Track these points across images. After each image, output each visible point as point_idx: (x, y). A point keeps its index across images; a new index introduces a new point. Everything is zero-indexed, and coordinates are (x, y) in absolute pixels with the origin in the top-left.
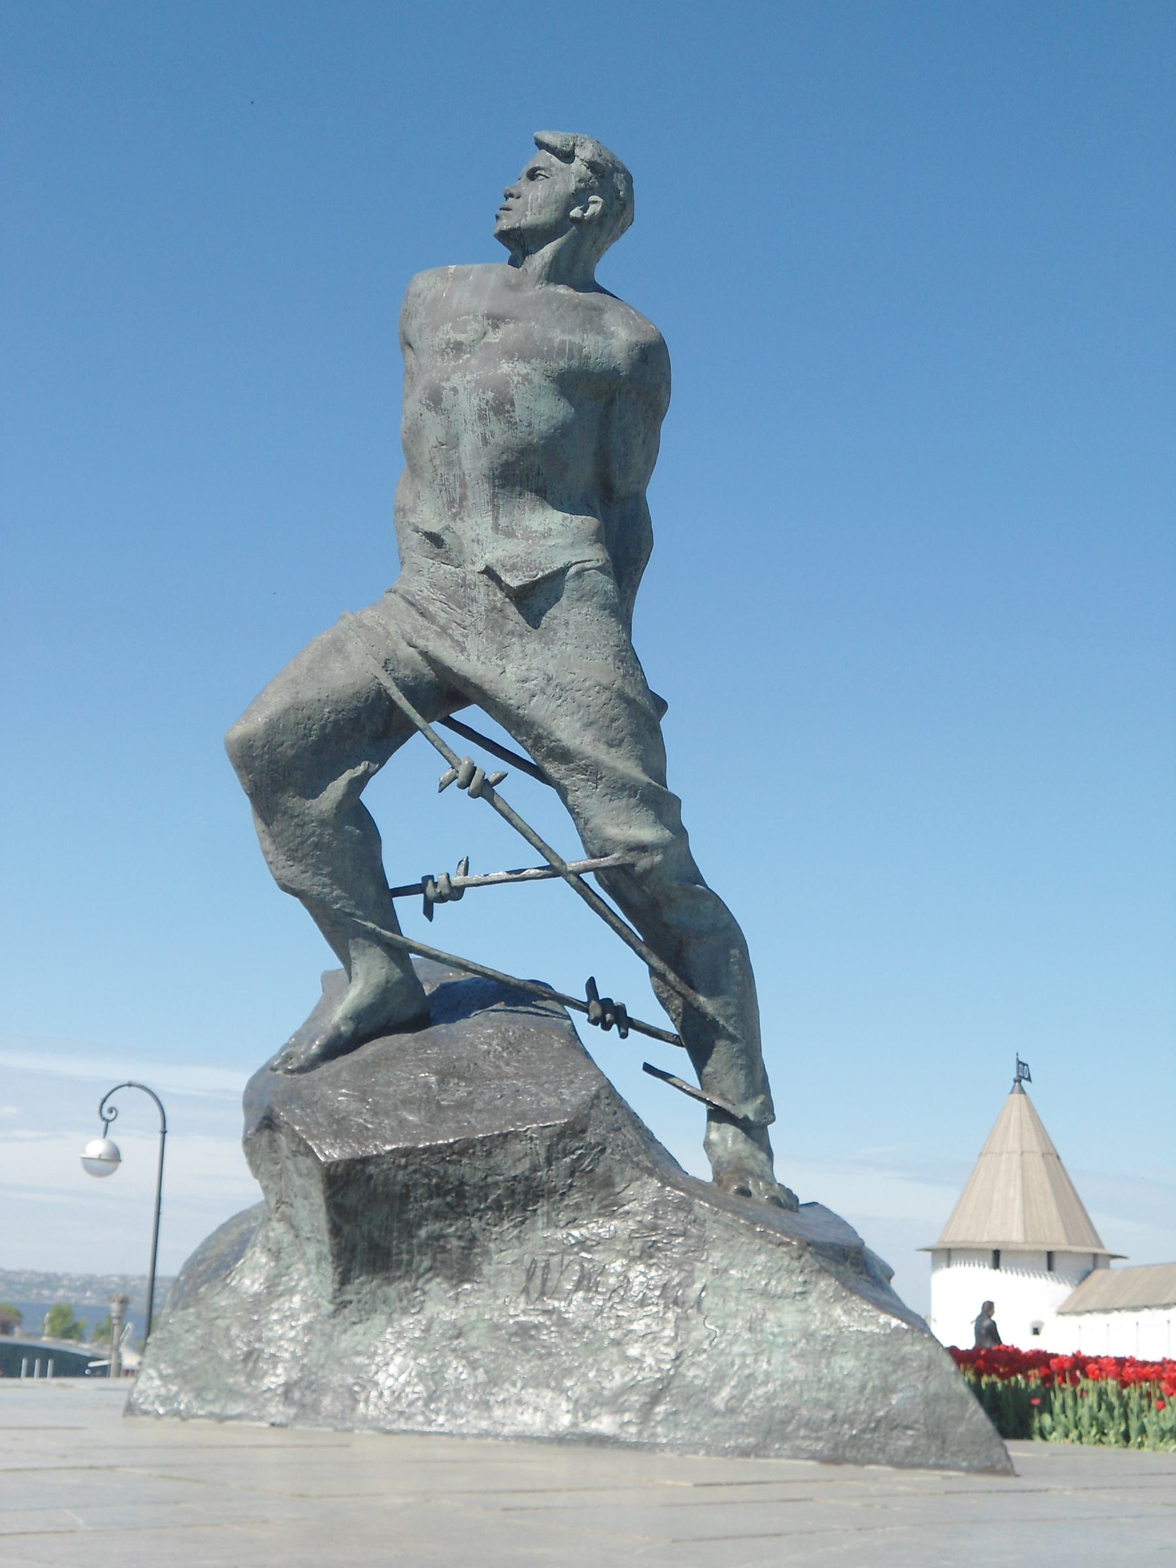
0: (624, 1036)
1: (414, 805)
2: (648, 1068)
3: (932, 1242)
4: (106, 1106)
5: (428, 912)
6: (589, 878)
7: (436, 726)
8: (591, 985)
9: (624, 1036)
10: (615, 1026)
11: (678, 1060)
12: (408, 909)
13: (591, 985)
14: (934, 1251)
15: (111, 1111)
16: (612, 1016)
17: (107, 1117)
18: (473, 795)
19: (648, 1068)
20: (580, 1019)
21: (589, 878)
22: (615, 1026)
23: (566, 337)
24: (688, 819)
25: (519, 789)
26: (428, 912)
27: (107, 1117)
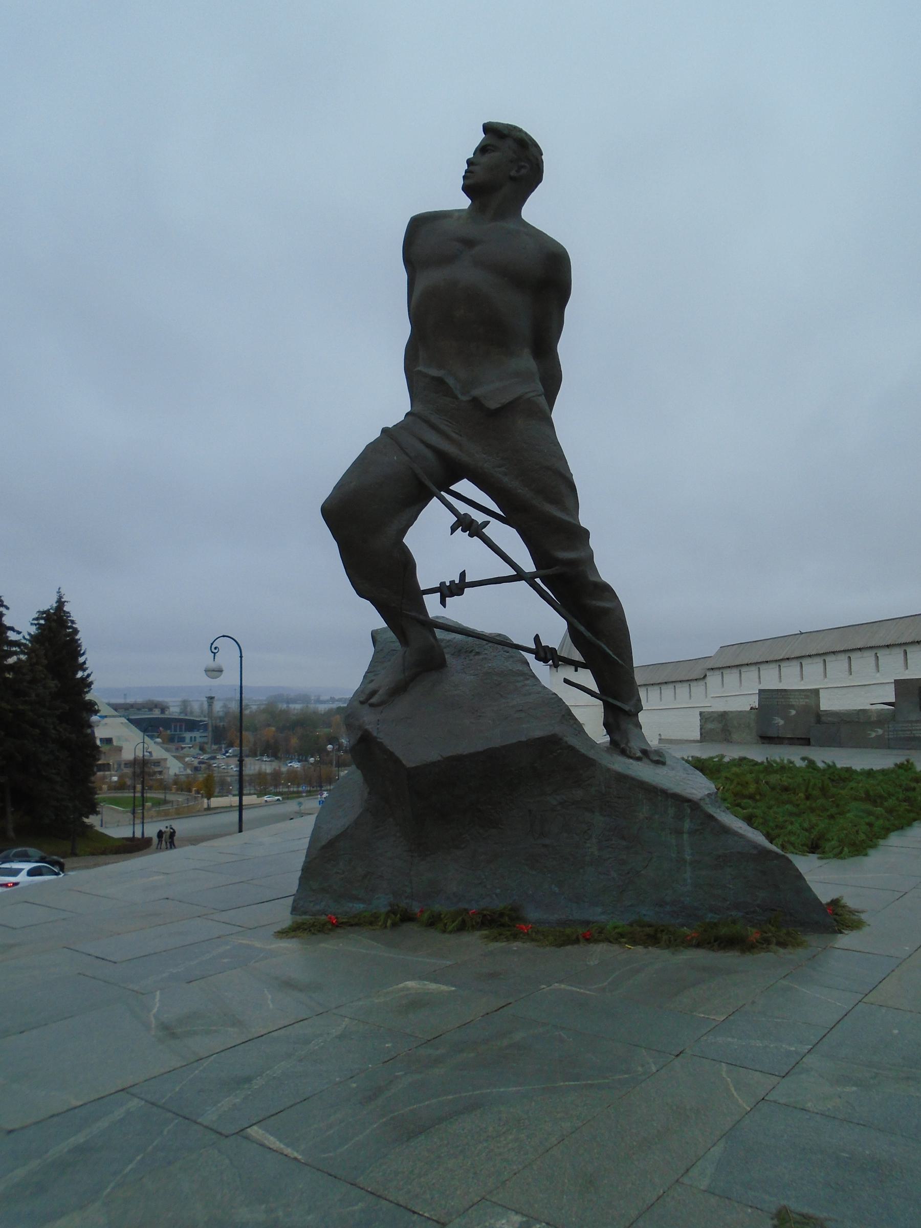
1: (435, 543)
4: (213, 646)
5: (443, 603)
6: (538, 580)
7: (442, 493)
8: (537, 639)
11: (586, 678)
13: (537, 639)
15: (215, 648)
17: (214, 650)
18: (471, 535)
19: (566, 681)
20: (530, 658)
21: (538, 580)
24: (593, 543)
26: (443, 603)
27: (214, 650)
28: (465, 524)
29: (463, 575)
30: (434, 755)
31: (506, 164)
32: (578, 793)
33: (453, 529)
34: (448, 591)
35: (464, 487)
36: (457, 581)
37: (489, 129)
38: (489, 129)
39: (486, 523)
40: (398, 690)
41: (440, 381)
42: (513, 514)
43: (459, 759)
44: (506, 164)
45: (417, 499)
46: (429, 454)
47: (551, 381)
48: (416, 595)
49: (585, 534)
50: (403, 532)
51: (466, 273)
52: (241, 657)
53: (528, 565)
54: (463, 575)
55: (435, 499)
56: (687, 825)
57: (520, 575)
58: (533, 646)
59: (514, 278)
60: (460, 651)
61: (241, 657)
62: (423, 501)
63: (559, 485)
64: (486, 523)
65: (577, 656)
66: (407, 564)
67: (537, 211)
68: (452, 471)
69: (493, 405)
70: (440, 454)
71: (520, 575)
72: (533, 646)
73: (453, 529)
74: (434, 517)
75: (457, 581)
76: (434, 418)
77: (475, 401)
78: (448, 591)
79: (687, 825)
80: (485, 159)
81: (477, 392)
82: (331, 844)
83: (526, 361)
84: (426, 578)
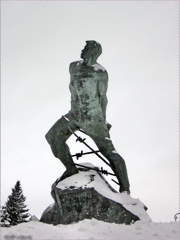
0: (107, 175)
2: (112, 180)
5: (77, 159)
6: (99, 153)
8: (102, 168)
9: (107, 175)
10: (106, 174)
11: (115, 178)
12: (74, 159)
13: (102, 168)
16: (106, 172)
19: (112, 180)
20: (101, 173)
22: (106, 174)
23: (90, 74)
24: (113, 143)
26: (77, 159)
28: (80, 139)
29: (82, 152)
33: (77, 141)
34: (79, 155)
36: (80, 153)
39: (85, 139)
45: (69, 134)
48: (71, 157)
50: (65, 140)
53: (96, 148)
54: (82, 152)
55: (73, 134)
57: (93, 152)
58: (101, 170)
64: (85, 139)
71: (93, 152)
72: (101, 170)
73: (77, 141)
75: (80, 153)
78: (79, 155)
84: (73, 152)
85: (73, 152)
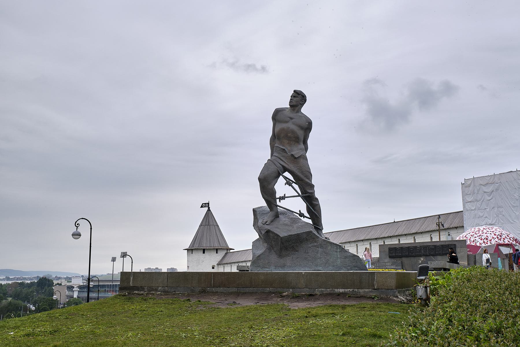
1: (281, 187)
3: (187, 247)
5: (280, 201)
8: (300, 211)
12: (278, 200)
13: (300, 211)
14: (188, 250)
16: (301, 215)
17: (77, 225)
20: (298, 215)
25: (294, 185)
26: (280, 201)
27: (77, 225)
30: (286, 234)
31: (299, 99)
32: (316, 244)
35: (287, 174)
37: (295, 91)
38: (295, 91)
40: (272, 221)
41: (284, 150)
42: (298, 180)
43: (291, 235)
44: (299, 99)
46: (281, 166)
47: (306, 149)
48: (275, 199)
49: (312, 186)
51: (290, 126)
52: (91, 229)
56: (338, 250)
57: (299, 196)
59: (301, 127)
60: (283, 213)
61: (91, 229)
62: (278, 177)
63: (309, 175)
65: (308, 216)
66: (274, 193)
67: (305, 110)
68: (285, 170)
69: (297, 156)
70: (283, 167)
74: (281, 180)
76: (282, 158)
77: (292, 155)
79: (338, 250)
80: (295, 99)
81: (293, 153)
82: (259, 256)
83: (302, 146)
85: (278, 196)
